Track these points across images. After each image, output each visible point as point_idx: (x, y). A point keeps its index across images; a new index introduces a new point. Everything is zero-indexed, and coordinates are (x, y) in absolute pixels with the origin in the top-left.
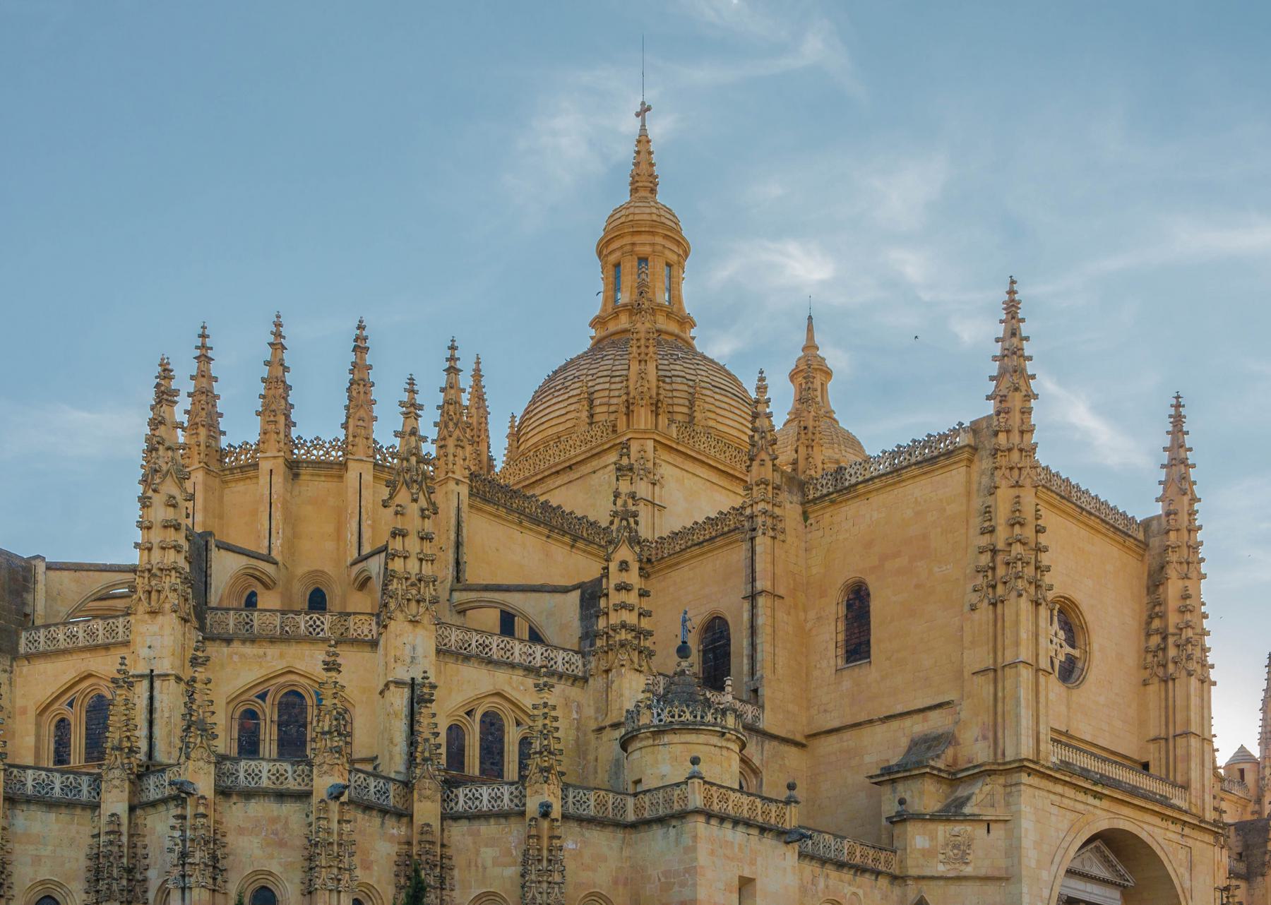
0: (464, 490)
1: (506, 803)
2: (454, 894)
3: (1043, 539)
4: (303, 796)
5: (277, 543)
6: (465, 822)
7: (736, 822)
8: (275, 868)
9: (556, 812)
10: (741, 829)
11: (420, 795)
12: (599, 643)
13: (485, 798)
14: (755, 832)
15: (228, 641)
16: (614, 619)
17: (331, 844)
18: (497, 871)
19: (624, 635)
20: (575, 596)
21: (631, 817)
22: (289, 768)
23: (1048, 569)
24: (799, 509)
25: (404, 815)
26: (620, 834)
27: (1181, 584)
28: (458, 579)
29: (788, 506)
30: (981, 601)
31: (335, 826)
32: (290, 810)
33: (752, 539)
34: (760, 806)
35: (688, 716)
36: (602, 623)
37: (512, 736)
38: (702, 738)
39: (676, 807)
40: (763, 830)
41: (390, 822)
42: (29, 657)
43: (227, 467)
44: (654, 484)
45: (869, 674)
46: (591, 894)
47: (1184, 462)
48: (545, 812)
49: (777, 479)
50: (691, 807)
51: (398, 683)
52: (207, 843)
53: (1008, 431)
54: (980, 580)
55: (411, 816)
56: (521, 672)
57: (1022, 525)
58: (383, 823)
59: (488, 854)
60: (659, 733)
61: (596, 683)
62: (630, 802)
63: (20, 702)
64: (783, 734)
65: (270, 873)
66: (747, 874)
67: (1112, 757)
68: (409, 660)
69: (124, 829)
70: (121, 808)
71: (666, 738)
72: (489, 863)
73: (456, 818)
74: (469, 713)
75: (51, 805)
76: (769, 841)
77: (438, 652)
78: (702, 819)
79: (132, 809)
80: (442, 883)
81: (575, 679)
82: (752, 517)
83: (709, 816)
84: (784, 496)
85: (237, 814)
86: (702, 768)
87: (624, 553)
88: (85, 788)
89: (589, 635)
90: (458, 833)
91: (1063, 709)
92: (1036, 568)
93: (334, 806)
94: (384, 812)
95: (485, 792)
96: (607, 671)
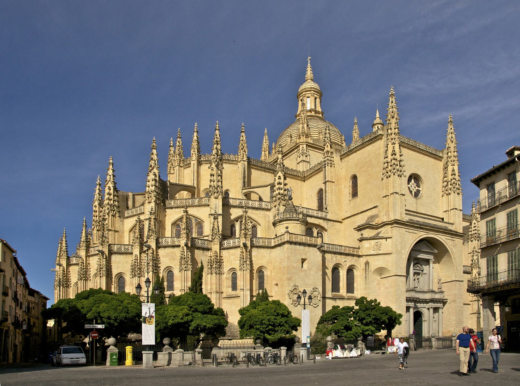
0: (246, 163)
1: (237, 244)
4: (179, 246)
7: (300, 244)
9: (249, 244)
12: (274, 199)
13: (231, 243)
15: (172, 208)
16: (277, 192)
17: (185, 258)
18: (235, 262)
19: (279, 196)
20: (269, 187)
21: (273, 245)
22: (175, 239)
26: (269, 250)
27: (452, 167)
28: (244, 186)
32: (176, 250)
36: (275, 193)
38: (292, 222)
39: (283, 241)
40: (310, 245)
42: (127, 218)
45: (358, 200)
48: (245, 245)
51: (212, 215)
52: (154, 260)
53: (391, 129)
57: (395, 155)
59: (232, 257)
60: (280, 222)
61: (274, 210)
62: (273, 240)
63: (125, 229)
64: (335, 219)
65: (171, 267)
69: (138, 258)
71: (283, 223)
72: (232, 260)
73: (224, 249)
79: (140, 253)
83: (291, 243)
87: (280, 174)
88: (130, 249)
89: (272, 197)
90: (224, 253)
91: (415, 205)
93: (185, 248)
95: (231, 241)
96: (275, 206)
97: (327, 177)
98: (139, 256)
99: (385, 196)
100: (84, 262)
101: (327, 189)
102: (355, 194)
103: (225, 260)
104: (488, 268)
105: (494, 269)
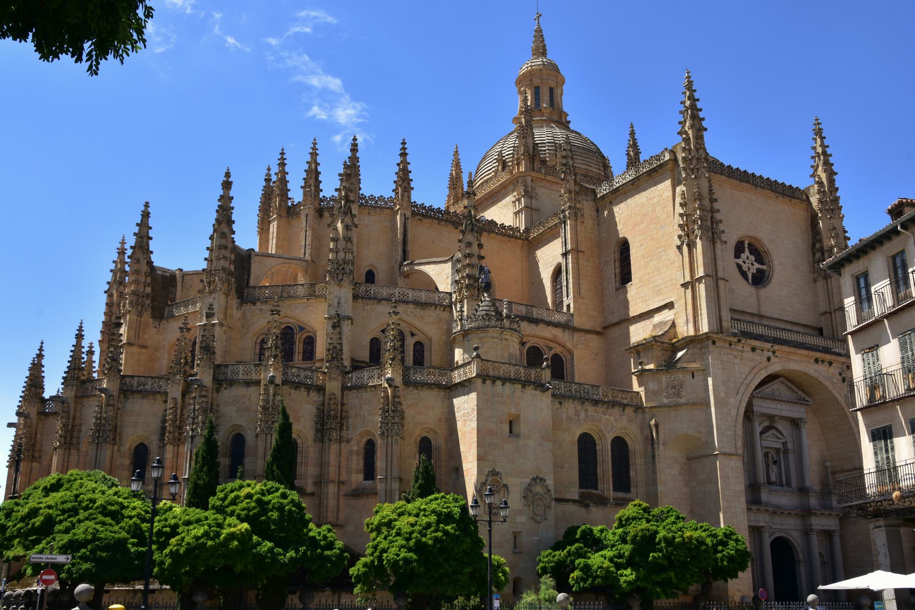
0: (409, 214)
2: (350, 431)
3: (716, 206)
5: (308, 252)
6: (355, 391)
7: (505, 380)
8: (242, 422)
10: (507, 384)
11: (330, 378)
14: (520, 386)
17: (267, 409)
23: (721, 221)
24: (592, 203)
25: (321, 389)
26: (442, 393)
29: (585, 203)
30: (682, 244)
31: (271, 397)
32: (252, 390)
33: (565, 223)
34: (523, 371)
35: (481, 323)
37: (410, 342)
43: (291, 212)
44: (532, 199)
46: (424, 428)
47: (824, 153)
49: (577, 188)
50: (474, 375)
54: (680, 233)
55: (325, 390)
56: (411, 306)
60: (464, 336)
65: (241, 426)
66: (513, 411)
67: (789, 327)
68: (336, 305)
69: (179, 405)
70: (178, 396)
73: (351, 389)
74: (383, 331)
75: (144, 394)
76: (530, 390)
77: (355, 297)
78: (479, 381)
80: (342, 426)
81: (445, 307)
82: (563, 211)
84: (580, 198)
85: (227, 394)
86: (480, 351)
92: (712, 223)
94: (309, 388)
97: (569, 241)
98: (179, 402)
99: (685, 285)
100: (72, 412)
101: (570, 266)
102: (625, 276)
103: (352, 413)
104: (876, 454)
105: (888, 458)
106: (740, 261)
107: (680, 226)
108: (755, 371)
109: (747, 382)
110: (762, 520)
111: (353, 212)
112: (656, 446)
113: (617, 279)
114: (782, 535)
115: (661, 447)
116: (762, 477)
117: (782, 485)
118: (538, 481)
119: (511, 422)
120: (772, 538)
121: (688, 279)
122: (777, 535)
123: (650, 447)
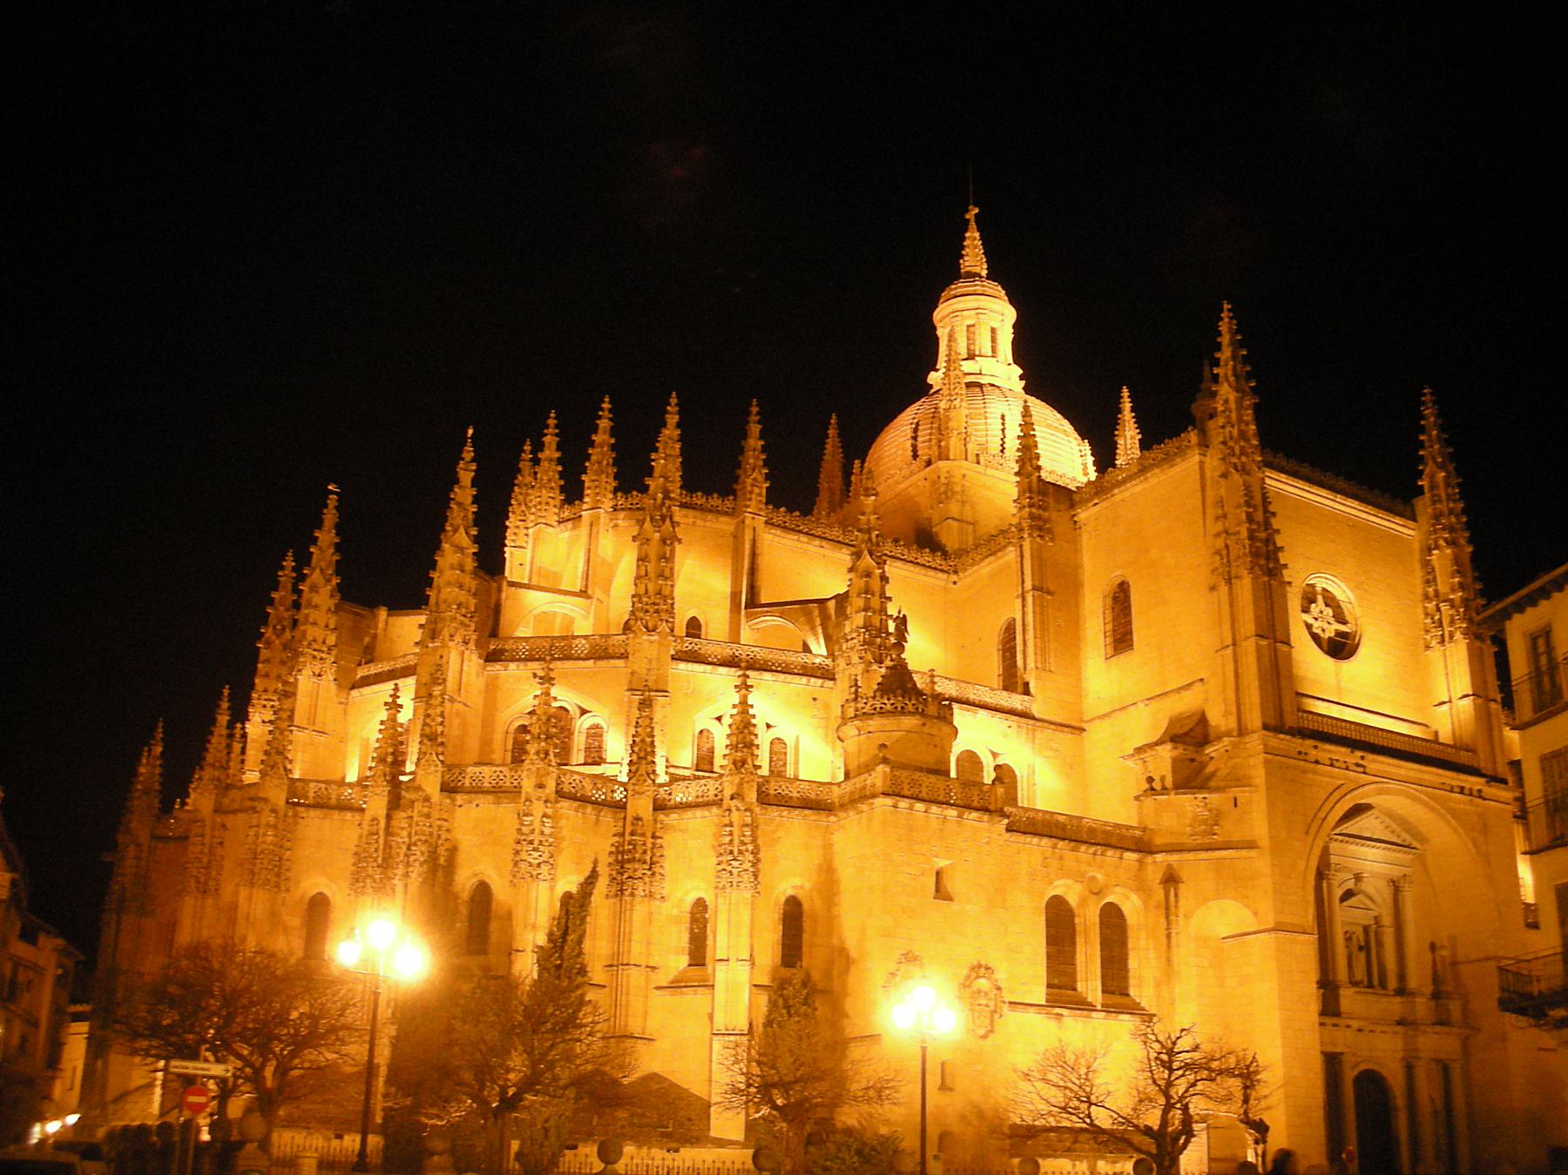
41: (607, 817)
58: (597, 820)
101: (1030, 618)
106: (1308, 618)
107: (1218, 553)
108: (1337, 794)
109: (1322, 814)
110: (1343, 1040)
111: (676, 519)
112: (1172, 918)
113: (1109, 640)
114: (1371, 1066)
115: (1181, 919)
116: (1342, 974)
117: (1370, 986)
118: (982, 971)
119: (938, 874)
120: (1356, 1072)
121: (1229, 641)
122: (1363, 1067)
123: (1163, 920)
